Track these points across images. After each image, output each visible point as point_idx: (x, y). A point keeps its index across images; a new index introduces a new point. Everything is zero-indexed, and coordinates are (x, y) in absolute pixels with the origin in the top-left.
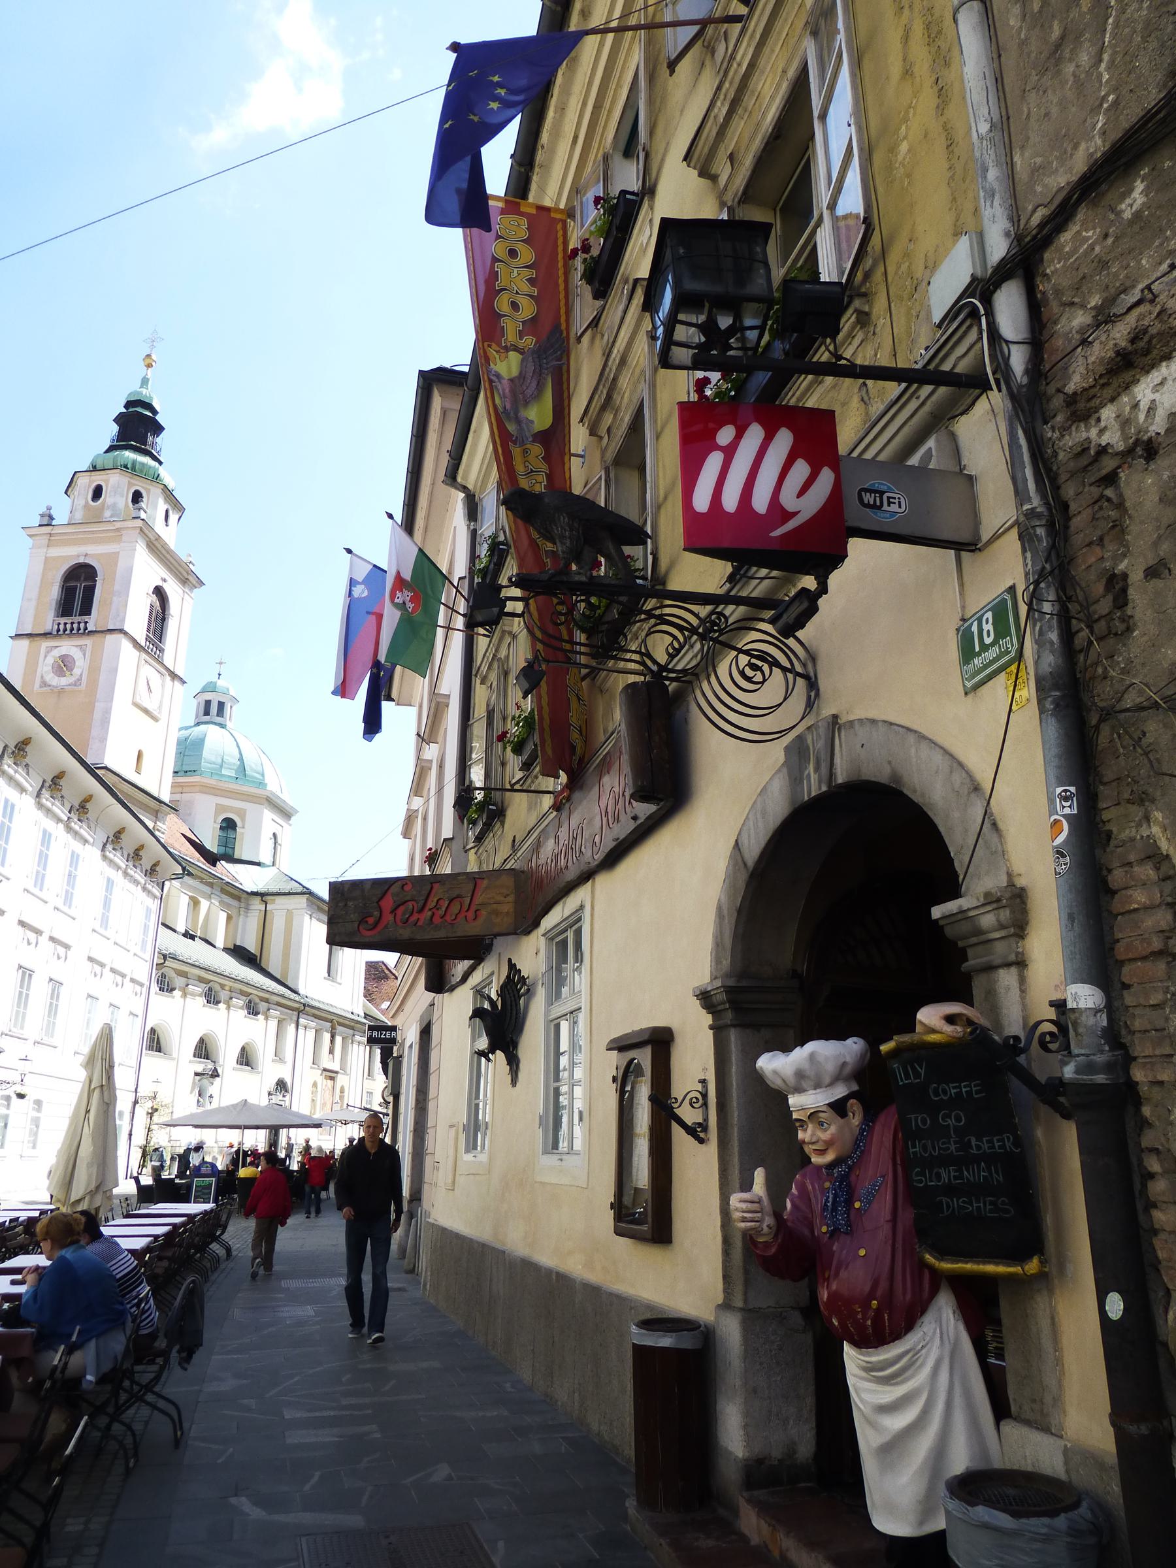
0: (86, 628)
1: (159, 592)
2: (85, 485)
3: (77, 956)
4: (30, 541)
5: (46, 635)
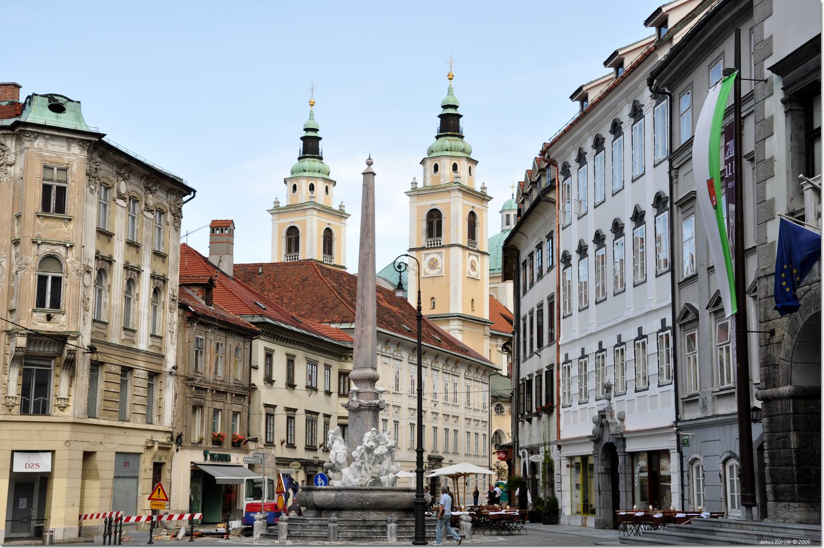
0: (440, 244)
1: (472, 214)
2: (430, 165)
3: (462, 421)
4: (408, 197)
5: (423, 249)
